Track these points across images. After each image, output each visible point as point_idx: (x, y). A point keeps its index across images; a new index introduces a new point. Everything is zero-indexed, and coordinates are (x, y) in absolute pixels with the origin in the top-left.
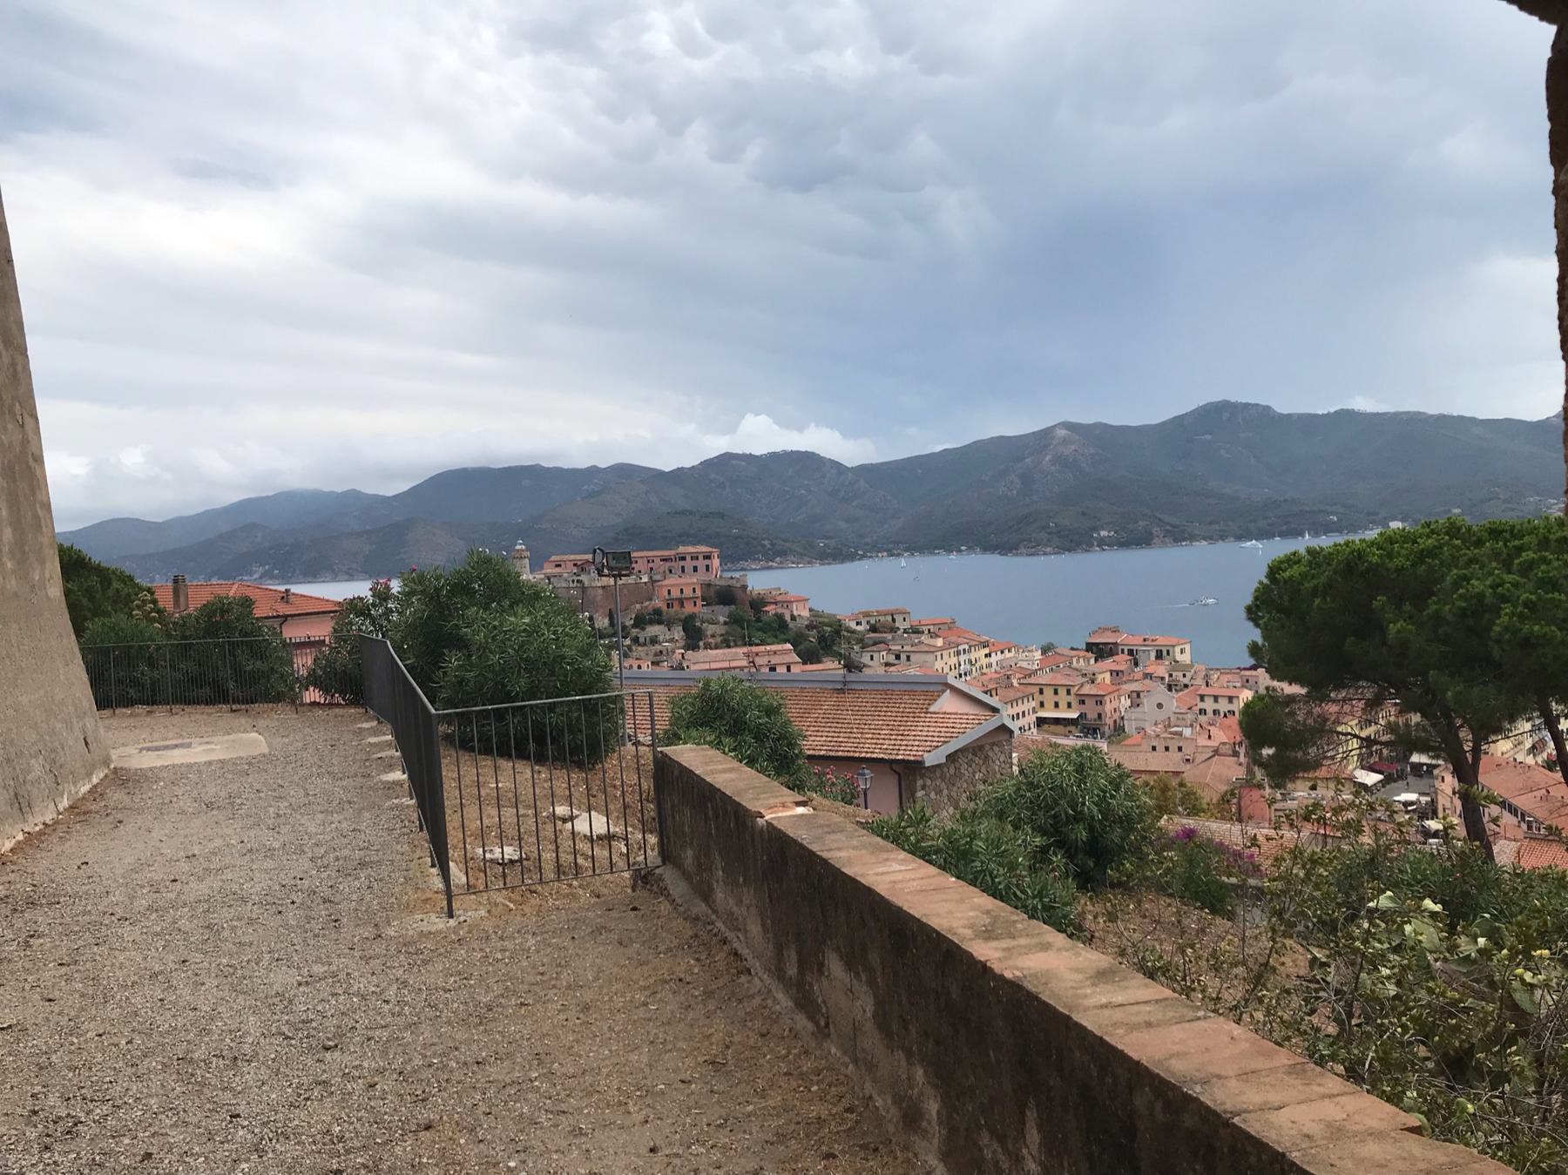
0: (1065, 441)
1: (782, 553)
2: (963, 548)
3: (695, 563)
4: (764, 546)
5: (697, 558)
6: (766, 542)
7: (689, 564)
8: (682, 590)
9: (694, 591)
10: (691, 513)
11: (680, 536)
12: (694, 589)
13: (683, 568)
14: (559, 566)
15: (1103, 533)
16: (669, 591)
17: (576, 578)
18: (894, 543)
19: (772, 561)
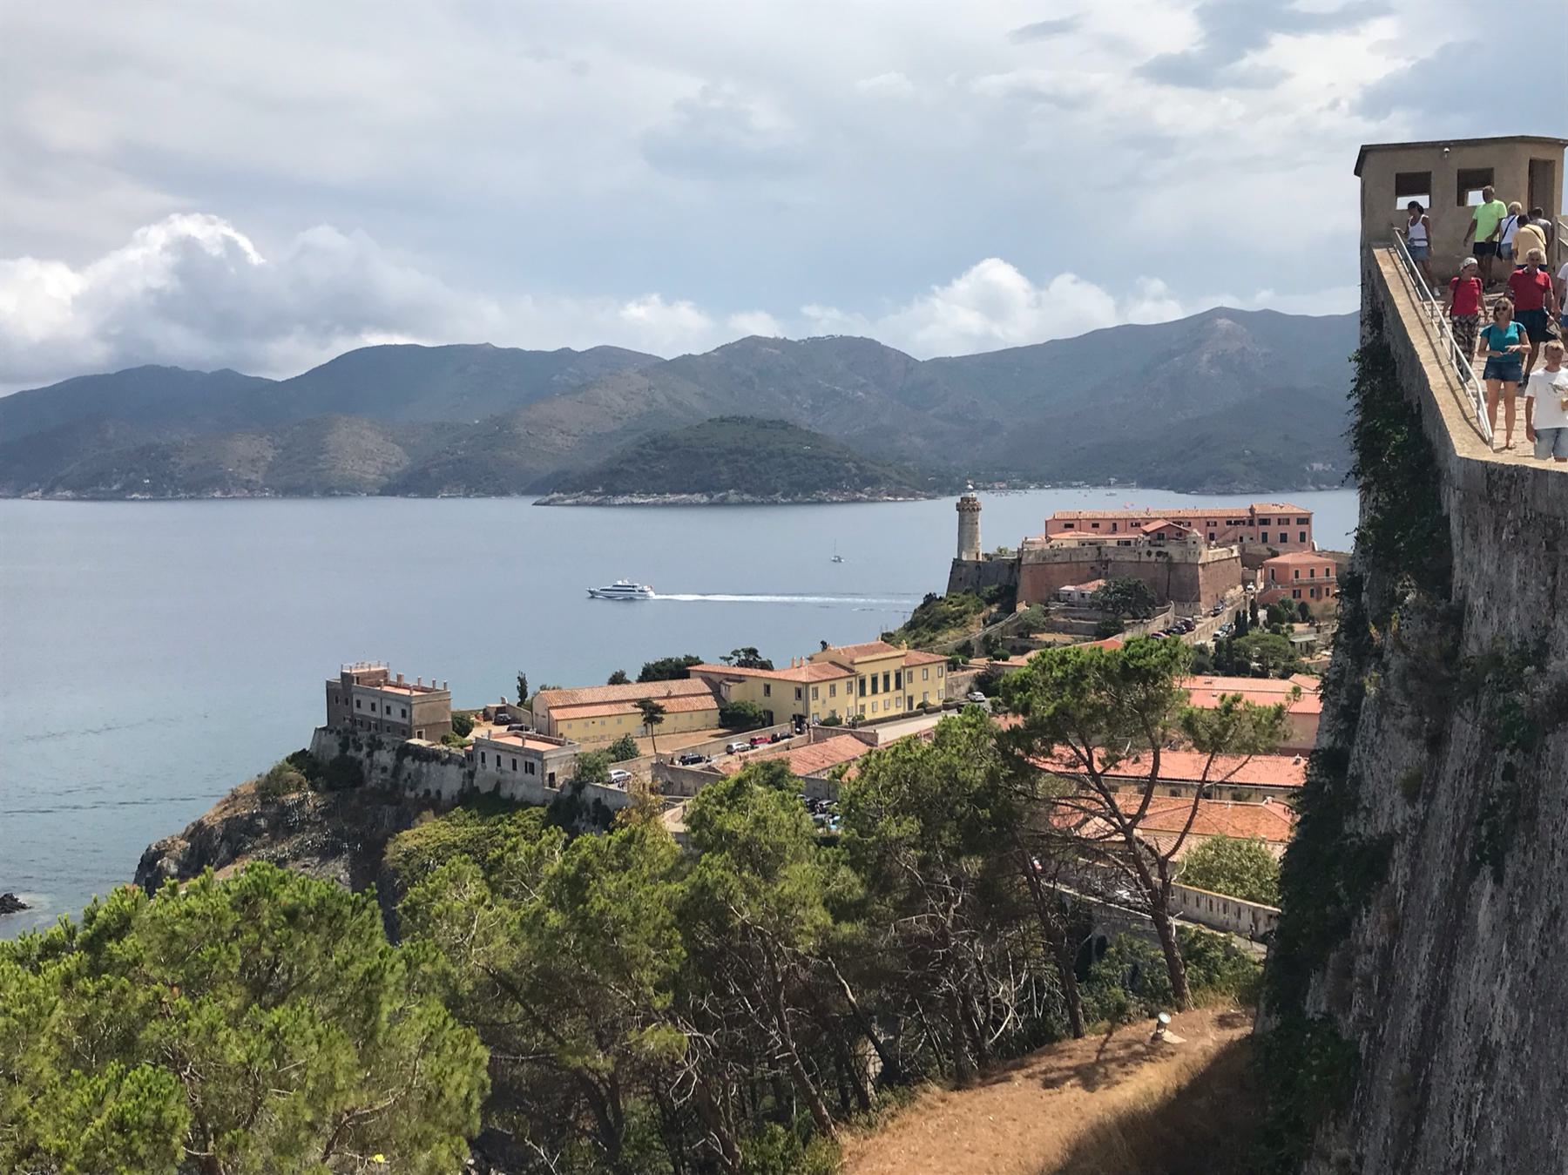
1: (872, 481)
2: (1113, 480)
3: (1283, 529)
4: (849, 471)
5: (1288, 522)
6: (850, 465)
7: (1274, 530)
8: (1312, 571)
9: (1328, 575)
10: (743, 420)
11: (730, 452)
12: (1328, 570)
13: (1265, 535)
14: (1071, 526)
15: (1318, 466)
16: (1297, 572)
17: (1154, 550)
19: (861, 492)
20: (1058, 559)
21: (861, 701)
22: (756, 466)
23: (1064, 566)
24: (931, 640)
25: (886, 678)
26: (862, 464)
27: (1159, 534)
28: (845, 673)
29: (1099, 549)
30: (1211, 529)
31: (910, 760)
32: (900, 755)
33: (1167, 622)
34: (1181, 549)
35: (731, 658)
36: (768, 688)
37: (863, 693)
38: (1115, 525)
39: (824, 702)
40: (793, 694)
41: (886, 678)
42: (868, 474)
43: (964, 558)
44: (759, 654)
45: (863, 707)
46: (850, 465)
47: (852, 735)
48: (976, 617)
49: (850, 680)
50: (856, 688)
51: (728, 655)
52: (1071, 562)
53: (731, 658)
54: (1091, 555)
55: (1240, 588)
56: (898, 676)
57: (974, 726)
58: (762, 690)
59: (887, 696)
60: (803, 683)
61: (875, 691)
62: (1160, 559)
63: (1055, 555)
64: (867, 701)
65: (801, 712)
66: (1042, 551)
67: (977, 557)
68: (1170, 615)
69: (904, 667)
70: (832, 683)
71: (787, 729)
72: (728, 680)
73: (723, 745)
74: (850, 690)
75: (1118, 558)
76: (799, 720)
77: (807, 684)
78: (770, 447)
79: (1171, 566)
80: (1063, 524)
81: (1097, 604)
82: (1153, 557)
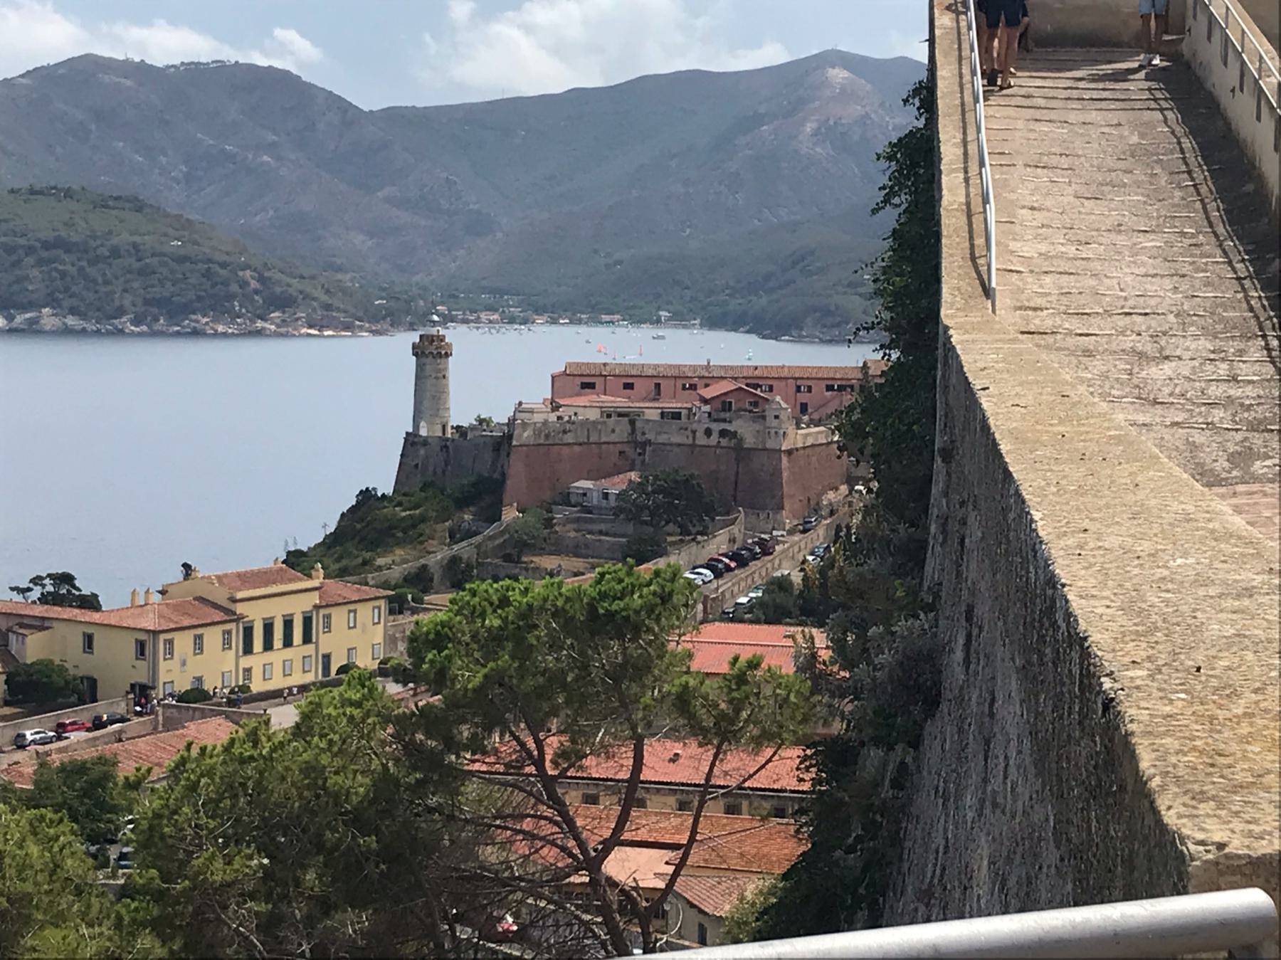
0: (846, 94)
1: (284, 302)
2: (663, 314)
4: (244, 284)
10: (69, 193)
11: (47, 245)
14: (591, 386)
17: (716, 427)
18: (492, 291)
20: (569, 438)
21: (246, 662)
22: (88, 270)
23: (577, 448)
24: (365, 563)
25: (288, 624)
26: (267, 274)
27: (724, 402)
28: (219, 616)
29: (632, 423)
30: (803, 397)
31: (252, 758)
32: (236, 750)
33: (732, 540)
34: (757, 427)
35: (29, 590)
36: (89, 641)
37: (248, 650)
38: (658, 386)
39: (184, 663)
40: (132, 649)
41: (288, 624)
42: (278, 290)
43: (423, 432)
44: (77, 583)
45: (248, 671)
46: (248, 273)
47: (227, 717)
48: (439, 527)
49: (227, 627)
50: (238, 640)
51: (24, 584)
52: (588, 443)
53: (29, 590)
54: (621, 431)
55: (844, 489)
56: (307, 621)
57: (358, 704)
58: (79, 642)
59: (288, 653)
60: (148, 631)
61: (268, 646)
62: (724, 442)
63: (565, 432)
64: (256, 661)
65: (144, 680)
66: (545, 423)
67: (444, 434)
68: (736, 530)
69: (317, 607)
70: (199, 631)
71: (121, 709)
72: (22, 626)
73: (11, 734)
74: (227, 644)
75: (662, 438)
76: (141, 693)
77: (155, 633)
78: (115, 241)
79: (741, 453)
80: (578, 381)
81: (626, 509)
82: (714, 439)
